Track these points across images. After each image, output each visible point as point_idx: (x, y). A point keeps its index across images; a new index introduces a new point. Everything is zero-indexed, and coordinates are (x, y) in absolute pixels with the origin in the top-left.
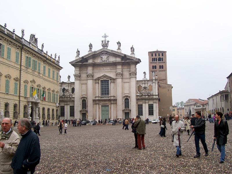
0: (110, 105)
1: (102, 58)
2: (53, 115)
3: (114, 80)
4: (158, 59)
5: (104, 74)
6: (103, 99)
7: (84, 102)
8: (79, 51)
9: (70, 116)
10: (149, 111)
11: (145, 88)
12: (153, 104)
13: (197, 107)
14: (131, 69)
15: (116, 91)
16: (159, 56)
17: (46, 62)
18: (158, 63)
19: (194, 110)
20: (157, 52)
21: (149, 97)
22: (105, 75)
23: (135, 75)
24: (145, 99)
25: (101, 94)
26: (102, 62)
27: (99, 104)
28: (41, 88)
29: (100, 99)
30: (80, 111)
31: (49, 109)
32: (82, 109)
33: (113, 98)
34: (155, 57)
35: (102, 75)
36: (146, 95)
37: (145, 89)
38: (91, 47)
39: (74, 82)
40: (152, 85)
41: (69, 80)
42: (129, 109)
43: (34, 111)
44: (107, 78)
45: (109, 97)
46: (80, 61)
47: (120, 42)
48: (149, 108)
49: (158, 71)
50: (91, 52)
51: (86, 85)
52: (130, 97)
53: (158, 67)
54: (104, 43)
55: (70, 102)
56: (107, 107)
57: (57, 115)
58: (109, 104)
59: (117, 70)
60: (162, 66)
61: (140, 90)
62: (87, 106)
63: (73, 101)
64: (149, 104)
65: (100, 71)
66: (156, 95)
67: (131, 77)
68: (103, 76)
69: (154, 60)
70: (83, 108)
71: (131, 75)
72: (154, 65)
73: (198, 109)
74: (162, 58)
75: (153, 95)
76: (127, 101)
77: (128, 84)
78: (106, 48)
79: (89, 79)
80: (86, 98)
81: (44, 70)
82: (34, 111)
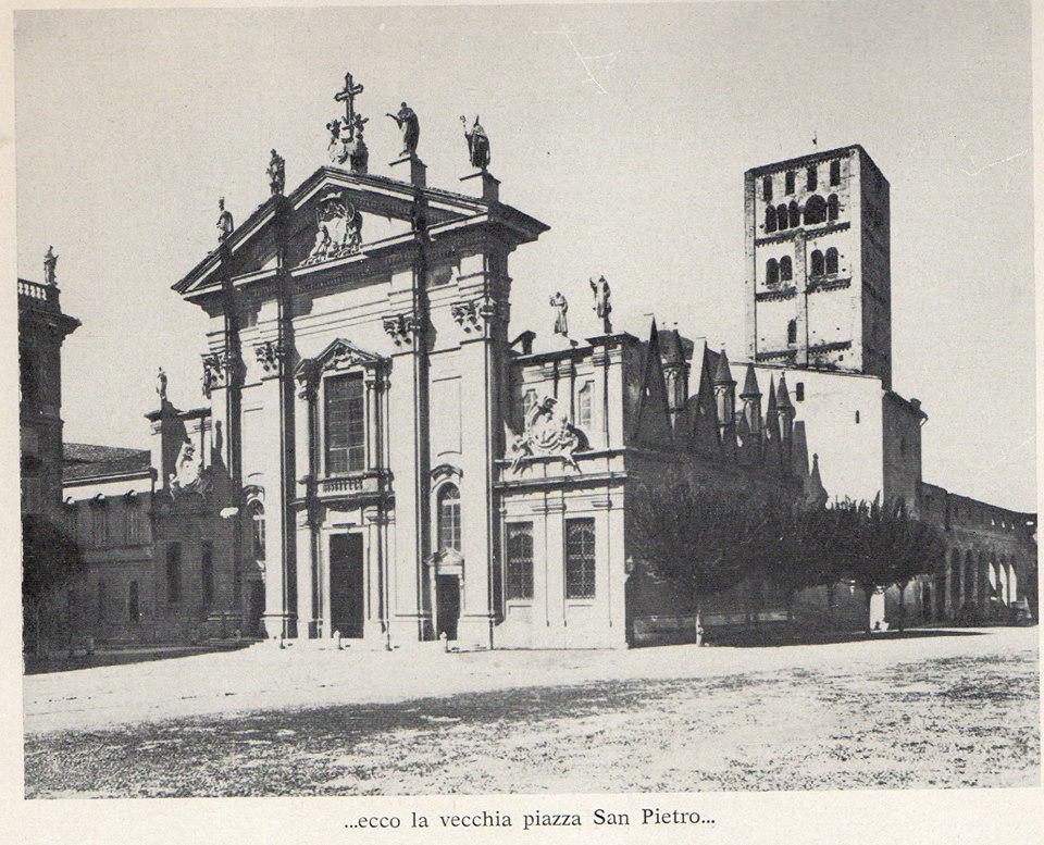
3: (383, 366)
34: (787, 201)
52: (461, 475)
60: (833, 253)
64: (569, 523)
66: (610, 455)
69: (780, 221)
72: (778, 251)
74: (834, 197)
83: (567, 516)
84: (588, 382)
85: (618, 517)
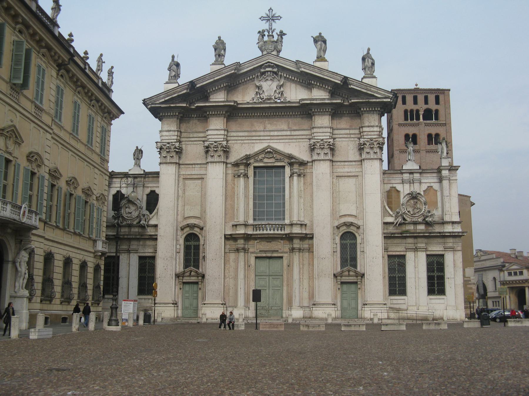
0: (285, 255)
1: (259, 87)
2: (83, 286)
4: (421, 113)
5: (266, 145)
6: (261, 232)
7: (192, 243)
8: (178, 65)
9: (138, 295)
10: (430, 278)
11: (414, 197)
12: (443, 256)
13: (510, 274)
14: (365, 129)
15: (312, 207)
16: (426, 102)
17: (68, 71)
18: (422, 127)
19: (498, 284)
20: (415, 93)
21: (430, 229)
22: (269, 147)
23: (378, 150)
24: (416, 236)
25: (254, 215)
26: (261, 103)
27: (245, 250)
28: (43, 172)
29: (250, 231)
30: (177, 276)
31: (68, 262)
32: (186, 266)
33: (300, 232)
34: (415, 107)
35: (258, 147)
36: (420, 223)
37: (412, 202)
38: (222, 52)
39: (158, 173)
40: (436, 186)
41: (138, 164)
42: (359, 269)
43: (10, 265)
44: (277, 160)
45: (283, 227)
46: (182, 98)
47: (322, 37)
48: (430, 268)
49: (423, 153)
50: (223, 66)
51: (200, 181)
53: (423, 139)
54: (266, 38)
55: (141, 243)
56: (275, 265)
57: (96, 287)
58: (287, 253)
59: (315, 130)
61: (393, 206)
62: (204, 257)
63: (154, 238)
64: (428, 256)
65: (254, 134)
66: (453, 223)
67: (364, 156)
68: (263, 151)
70: (187, 263)
71: (366, 150)
72: (411, 131)
73: (513, 281)
74: (437, 111)
75: (443, 223)
76: (348, 242)
77: (352, 181)
78: (275, 53)
79: (211, 162)
80: (202, 229)
81: (59, 103)
82: (10, 265)
83: (428, 253)
84: (428, 187)
85: (459, 255)
